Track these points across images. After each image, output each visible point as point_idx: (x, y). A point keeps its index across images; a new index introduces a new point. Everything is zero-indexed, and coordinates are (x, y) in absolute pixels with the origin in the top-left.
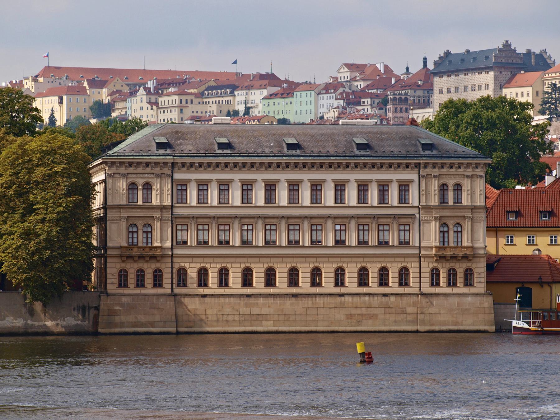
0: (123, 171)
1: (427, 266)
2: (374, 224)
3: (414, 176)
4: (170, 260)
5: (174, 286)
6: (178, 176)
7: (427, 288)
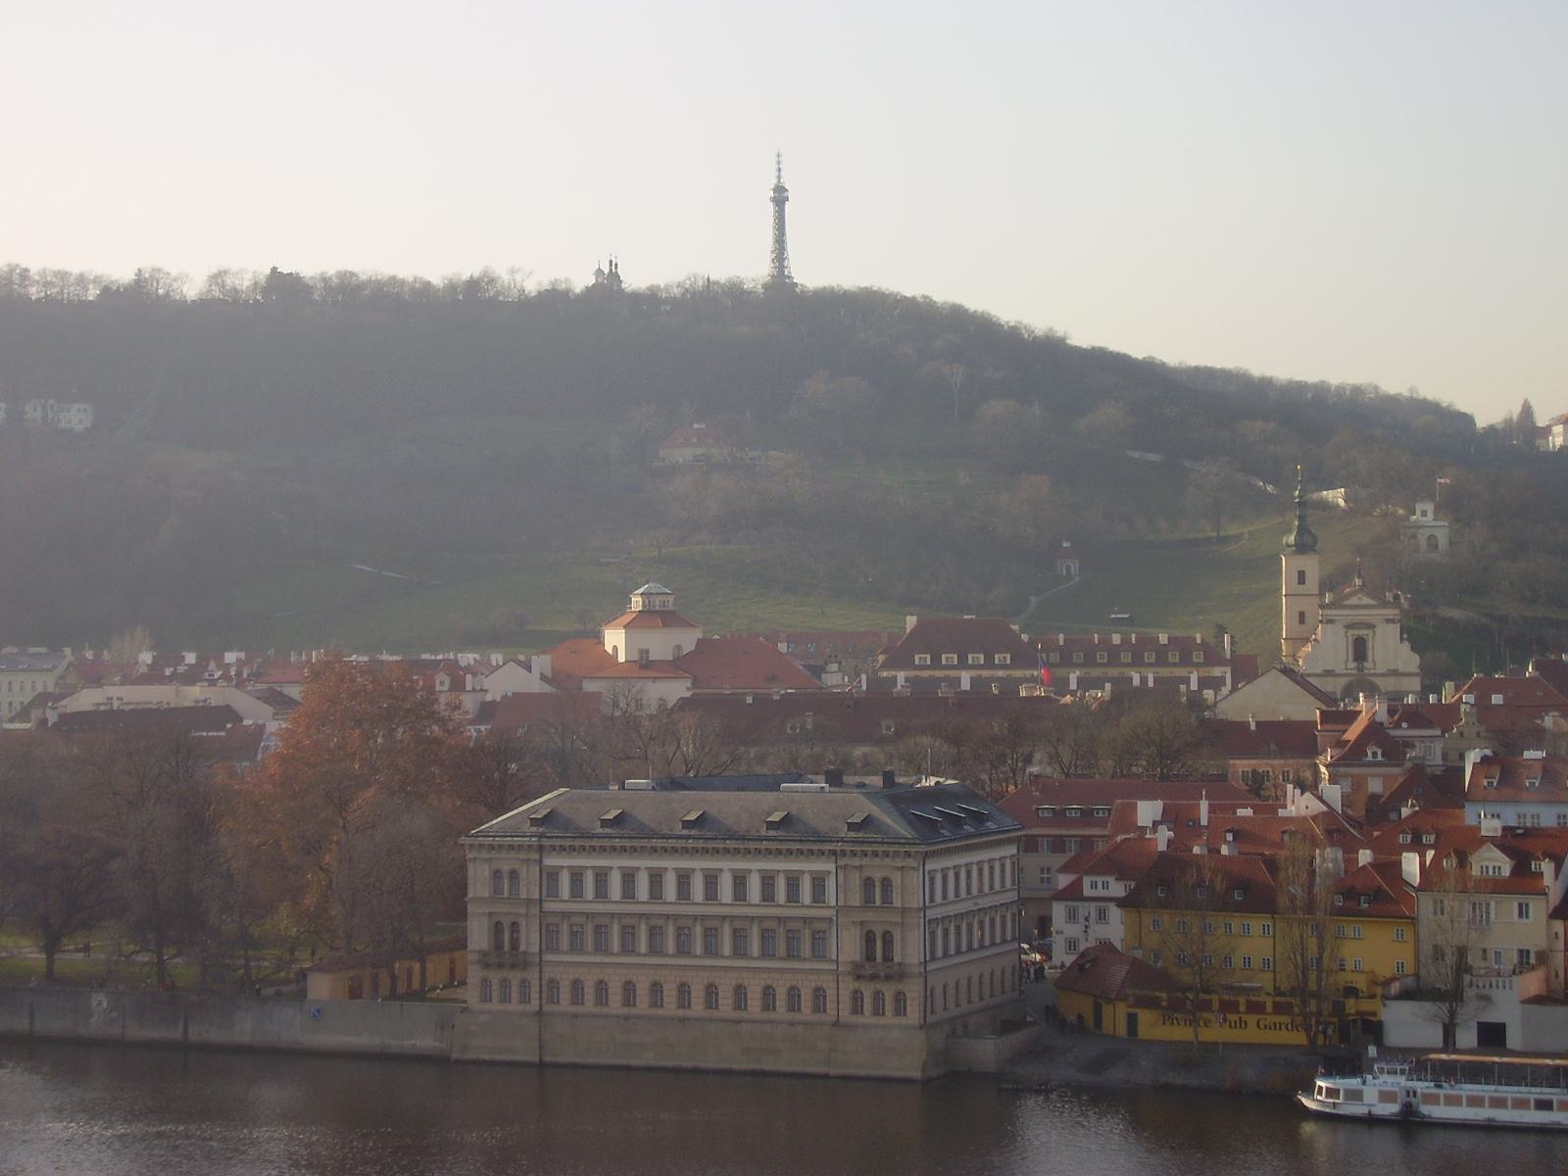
0: (484, 855)
1: (848, 986)
2: (781, 930)
3: (830, 867)
4: (538, 969)
5: (544, 1001)
6: (551, 861)
7: (845, 1015)
